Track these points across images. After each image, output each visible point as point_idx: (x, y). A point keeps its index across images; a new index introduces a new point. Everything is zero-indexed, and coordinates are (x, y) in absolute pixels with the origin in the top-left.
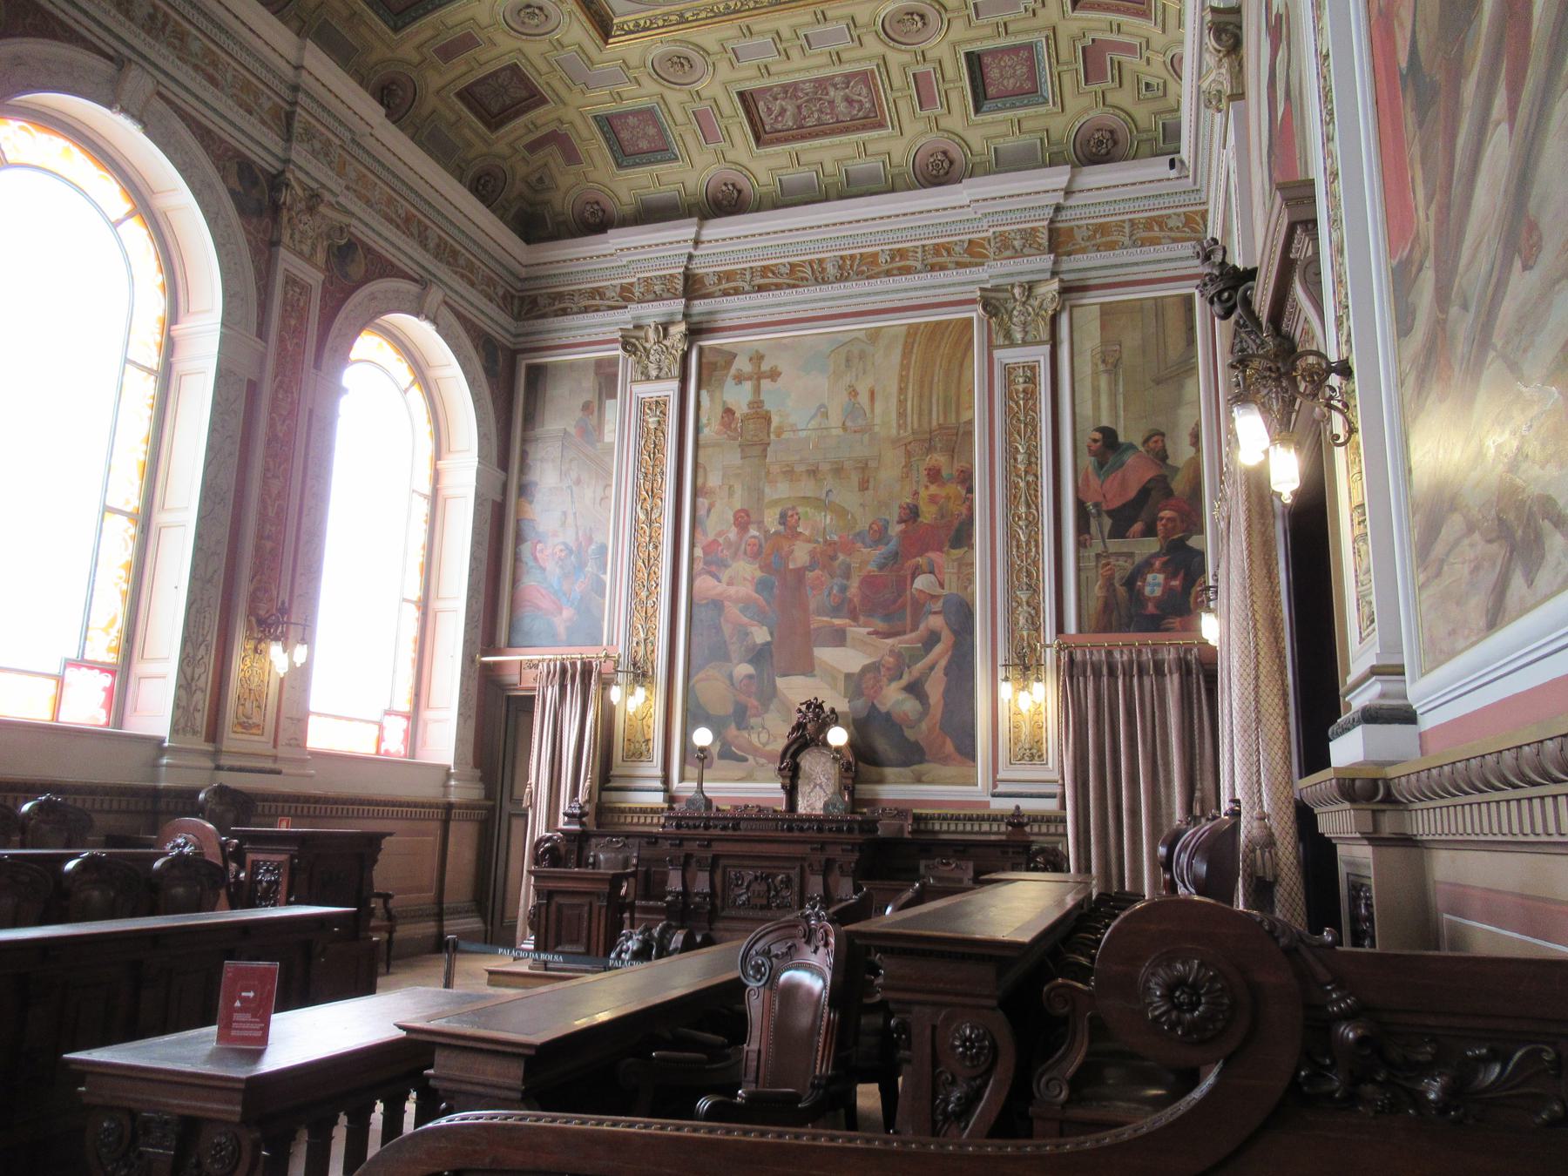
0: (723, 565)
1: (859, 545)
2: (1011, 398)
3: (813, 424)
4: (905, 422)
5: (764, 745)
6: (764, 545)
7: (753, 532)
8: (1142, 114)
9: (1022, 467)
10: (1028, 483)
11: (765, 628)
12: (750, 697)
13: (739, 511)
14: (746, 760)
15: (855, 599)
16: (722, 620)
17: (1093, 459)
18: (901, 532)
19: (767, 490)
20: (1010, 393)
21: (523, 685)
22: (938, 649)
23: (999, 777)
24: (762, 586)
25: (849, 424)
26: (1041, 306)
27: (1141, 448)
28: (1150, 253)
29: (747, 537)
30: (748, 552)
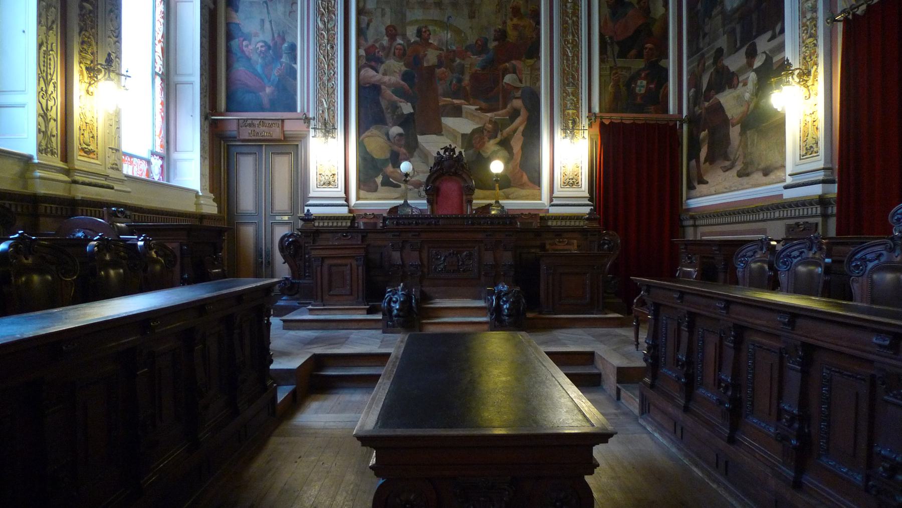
0: (380, 61)
1: (469, 53)
6: (406, 48)
7: (399, 41)
9: (570, 11)
10: (573, 21)
11: (409, 104)
12: (401, 147)
15: (467, 87)
16: (380, 99)
17: (609, 9)
18: (495, 46)
21: (242, 137)
22: (518, 120)
23: (554, 195)
24: (405, 77)
27: (637, 6)
29: (395, 44)
30: (397, 54)
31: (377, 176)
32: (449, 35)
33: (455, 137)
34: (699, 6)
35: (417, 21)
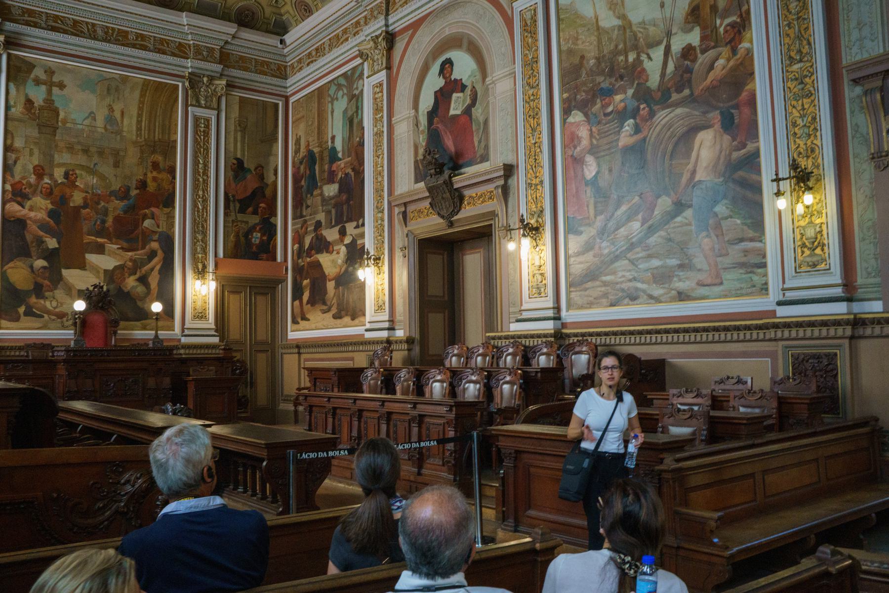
0: (26, 197)
1: (113, 198)
2: (197, 133)
3: (87, 122)
4: (141, 133)
5: (55, 308)
7: (47, 180)
8: (268, 11)
9: (201, 171)
10: (204, 180)
13: (36, 166)
14: (43, 317)
15: (111, 229)
16: (25, 232)
18: (137, 194)
19: (56, 156)
20: (197, 131)
22: (156, 260)
24: (52, 214)
25: (108, 127)
26: (215, 90)
28: (263, 78)
31: (20, 306)
32: (95, 181)
33: (98, 272)
34: (303, 183)
35: (64, 164)
